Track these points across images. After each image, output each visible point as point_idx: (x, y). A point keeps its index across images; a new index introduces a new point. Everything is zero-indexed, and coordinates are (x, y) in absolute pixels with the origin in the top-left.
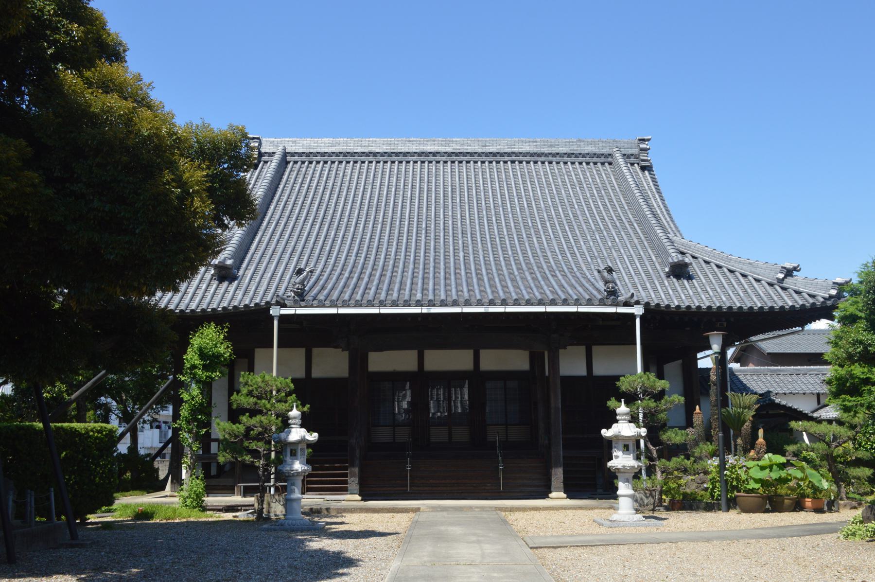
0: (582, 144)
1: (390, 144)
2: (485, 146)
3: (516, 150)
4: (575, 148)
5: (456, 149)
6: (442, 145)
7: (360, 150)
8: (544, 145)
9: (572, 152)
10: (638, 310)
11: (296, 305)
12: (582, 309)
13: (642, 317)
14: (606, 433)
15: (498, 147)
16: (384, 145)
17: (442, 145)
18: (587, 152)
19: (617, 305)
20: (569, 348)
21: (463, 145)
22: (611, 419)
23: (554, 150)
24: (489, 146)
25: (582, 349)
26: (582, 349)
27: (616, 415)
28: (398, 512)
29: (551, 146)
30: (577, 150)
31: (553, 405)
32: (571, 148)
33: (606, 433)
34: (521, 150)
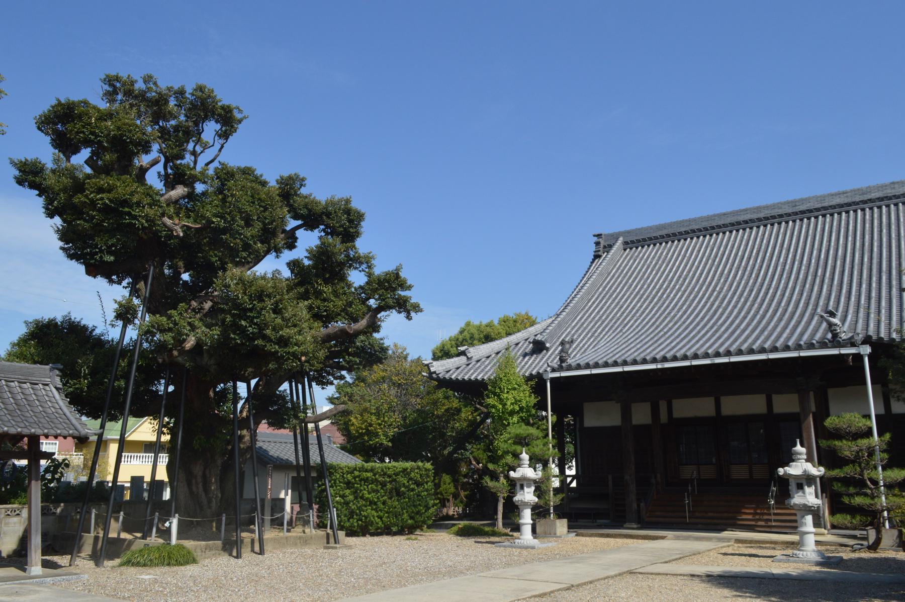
0: (896, 186)
1: (708, 220)
2: (796, 206)
3: (826, 204)
4: (889, 191)
5: (768, 214)
6: (754, 212)
7: (683, 230)
8: (855, 194)
9: (885, 195)
10: (866, 350)
11: (560, 368)
12: (804, 354)
13: (870, 356)
14: (781, 471)
15: (808, 205)
16: (702, 222)
17: (754, 212)
18: (901, 193)
19: (840, 345)
21: (774, 209)
22: (788, 459)
23: (866, 197)
24: (799, 205)
29: (863, 194)
30: (891, 193)
32: (885, 192)
34: (831, 204)
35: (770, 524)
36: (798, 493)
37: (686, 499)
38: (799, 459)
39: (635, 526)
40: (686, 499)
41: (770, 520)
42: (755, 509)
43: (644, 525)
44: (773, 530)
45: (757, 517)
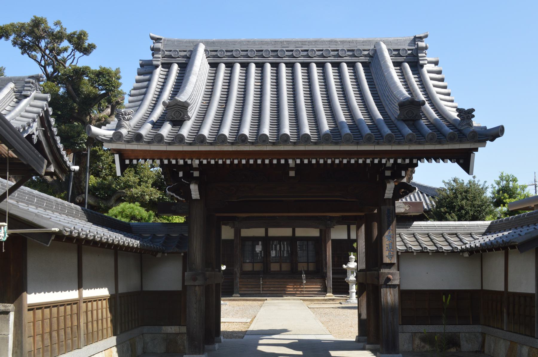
20: (335, 227)
22: (347, 261)
25: (346, 226)
26: (346, 226)
27: (349, 259)
28: (257, 301)
31: (328, 254)
33: (344, 266)
35: (302, 292)
36: (351, 275)
37: (261, 281)
38: (352, 261)
39: (239, 295)
40: (261, 281)
41: (303, 291)
42: (293, 286)
43: (242, 295)
44: (304, 295)
45: (295, 290)
